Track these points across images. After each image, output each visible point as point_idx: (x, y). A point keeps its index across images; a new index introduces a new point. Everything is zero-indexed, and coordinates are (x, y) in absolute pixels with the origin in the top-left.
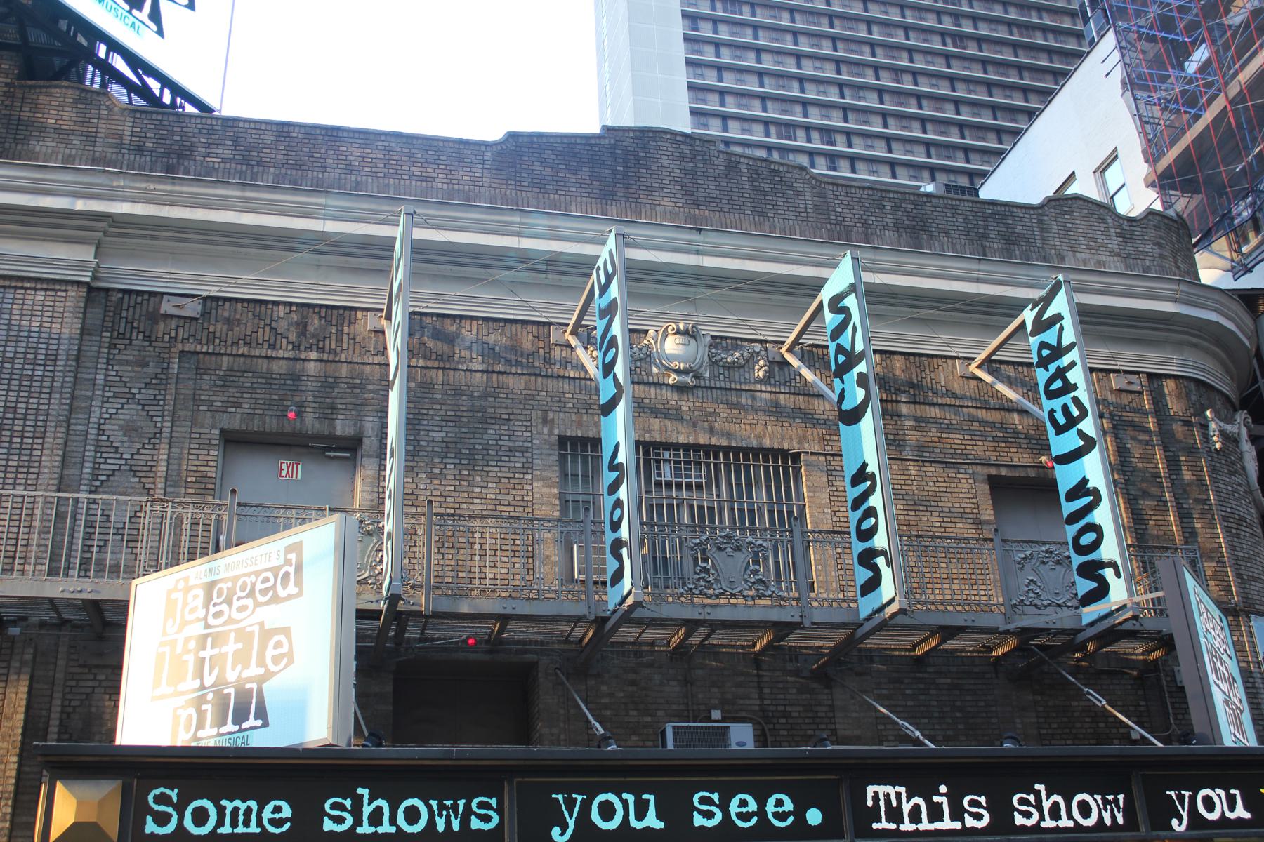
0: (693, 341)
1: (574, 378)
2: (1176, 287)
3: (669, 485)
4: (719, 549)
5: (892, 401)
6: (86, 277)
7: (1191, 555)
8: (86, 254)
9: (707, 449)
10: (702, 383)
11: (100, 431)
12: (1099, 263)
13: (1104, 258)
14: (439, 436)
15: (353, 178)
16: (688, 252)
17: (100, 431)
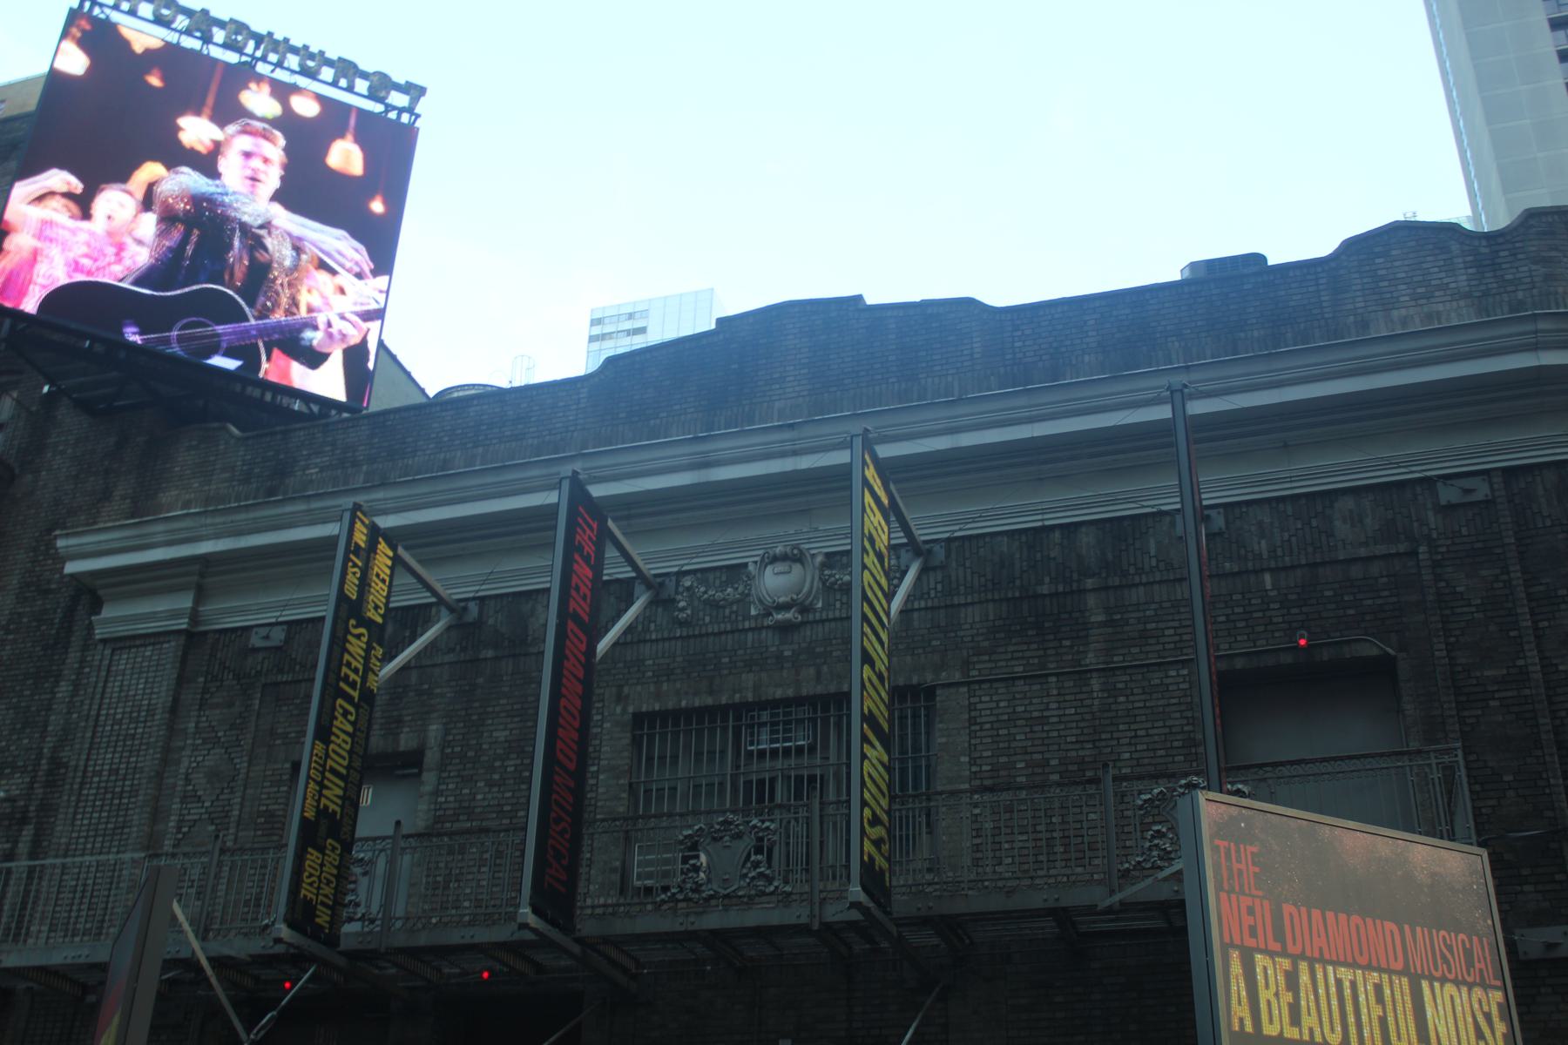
0: (797, 568)
1: (657, 640)
2: (1529, 327)
3: (762, 753)
4: (715, 839)
5: (1072, 592)
6: (183, 624)
7: (1446, 759)
8: (185, 602)
9: (812, 701)
10: (811, 617)
11: (188, 780)
12: (1429, 317)
13: (1440, 307)
14: (501, 735)
15: (442, 456)
16: (783, 455)
17: (188, 780)
